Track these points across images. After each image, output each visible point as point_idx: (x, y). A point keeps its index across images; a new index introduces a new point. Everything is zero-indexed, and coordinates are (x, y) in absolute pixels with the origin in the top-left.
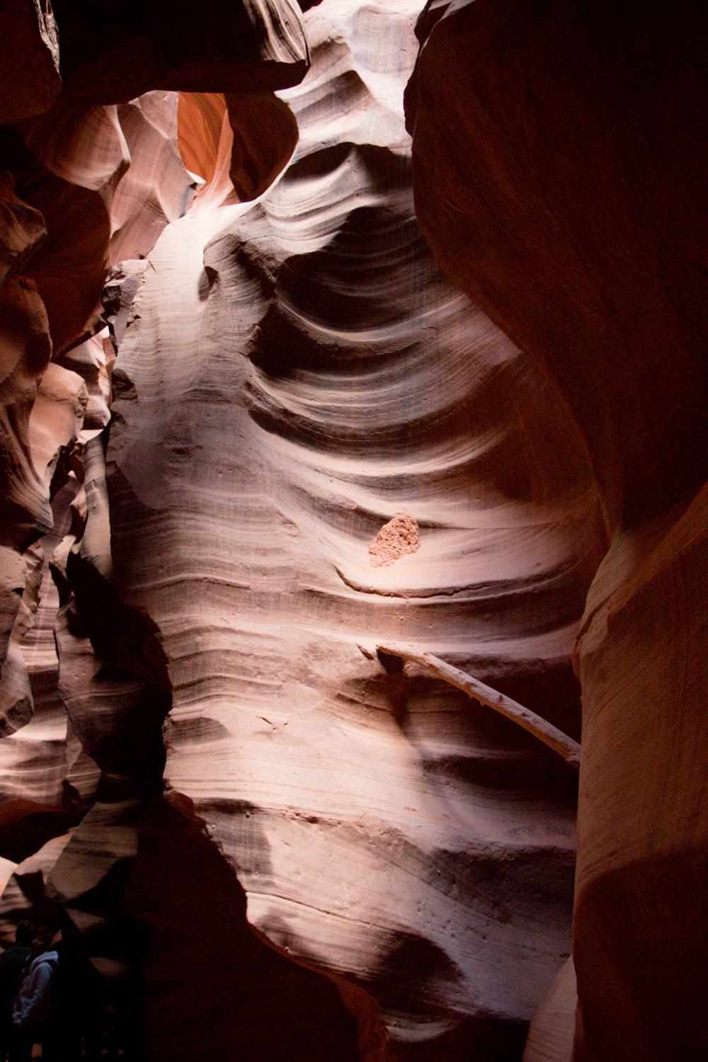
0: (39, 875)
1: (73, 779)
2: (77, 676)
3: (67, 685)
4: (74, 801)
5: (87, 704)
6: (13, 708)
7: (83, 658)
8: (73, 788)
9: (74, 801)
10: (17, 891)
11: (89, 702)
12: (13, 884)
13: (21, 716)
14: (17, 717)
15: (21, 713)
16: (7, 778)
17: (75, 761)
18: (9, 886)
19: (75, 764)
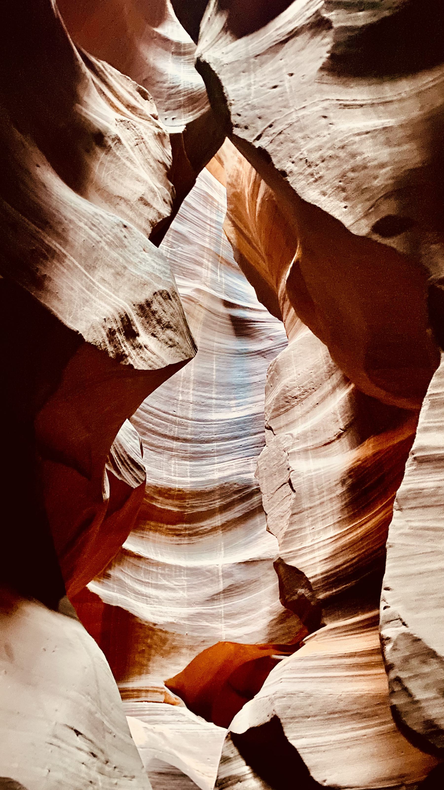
0: (274, 726)
1: (291, 555)
2: (275, 87)
3: (253, 107)
4: (301, 591)
5: (324, 121)
6: (149, 304)
7: (279, 55)
8: (294, 569)
9: (301, 591)
10: (241, 767)
11: (325, 117)
12: (232, 756)
13: (169, 332)
14: (162, 336)
15: (168, 327)
16: (200, 615)
17: (285, 530)
18: (225, 760)
19: (286, 534)
